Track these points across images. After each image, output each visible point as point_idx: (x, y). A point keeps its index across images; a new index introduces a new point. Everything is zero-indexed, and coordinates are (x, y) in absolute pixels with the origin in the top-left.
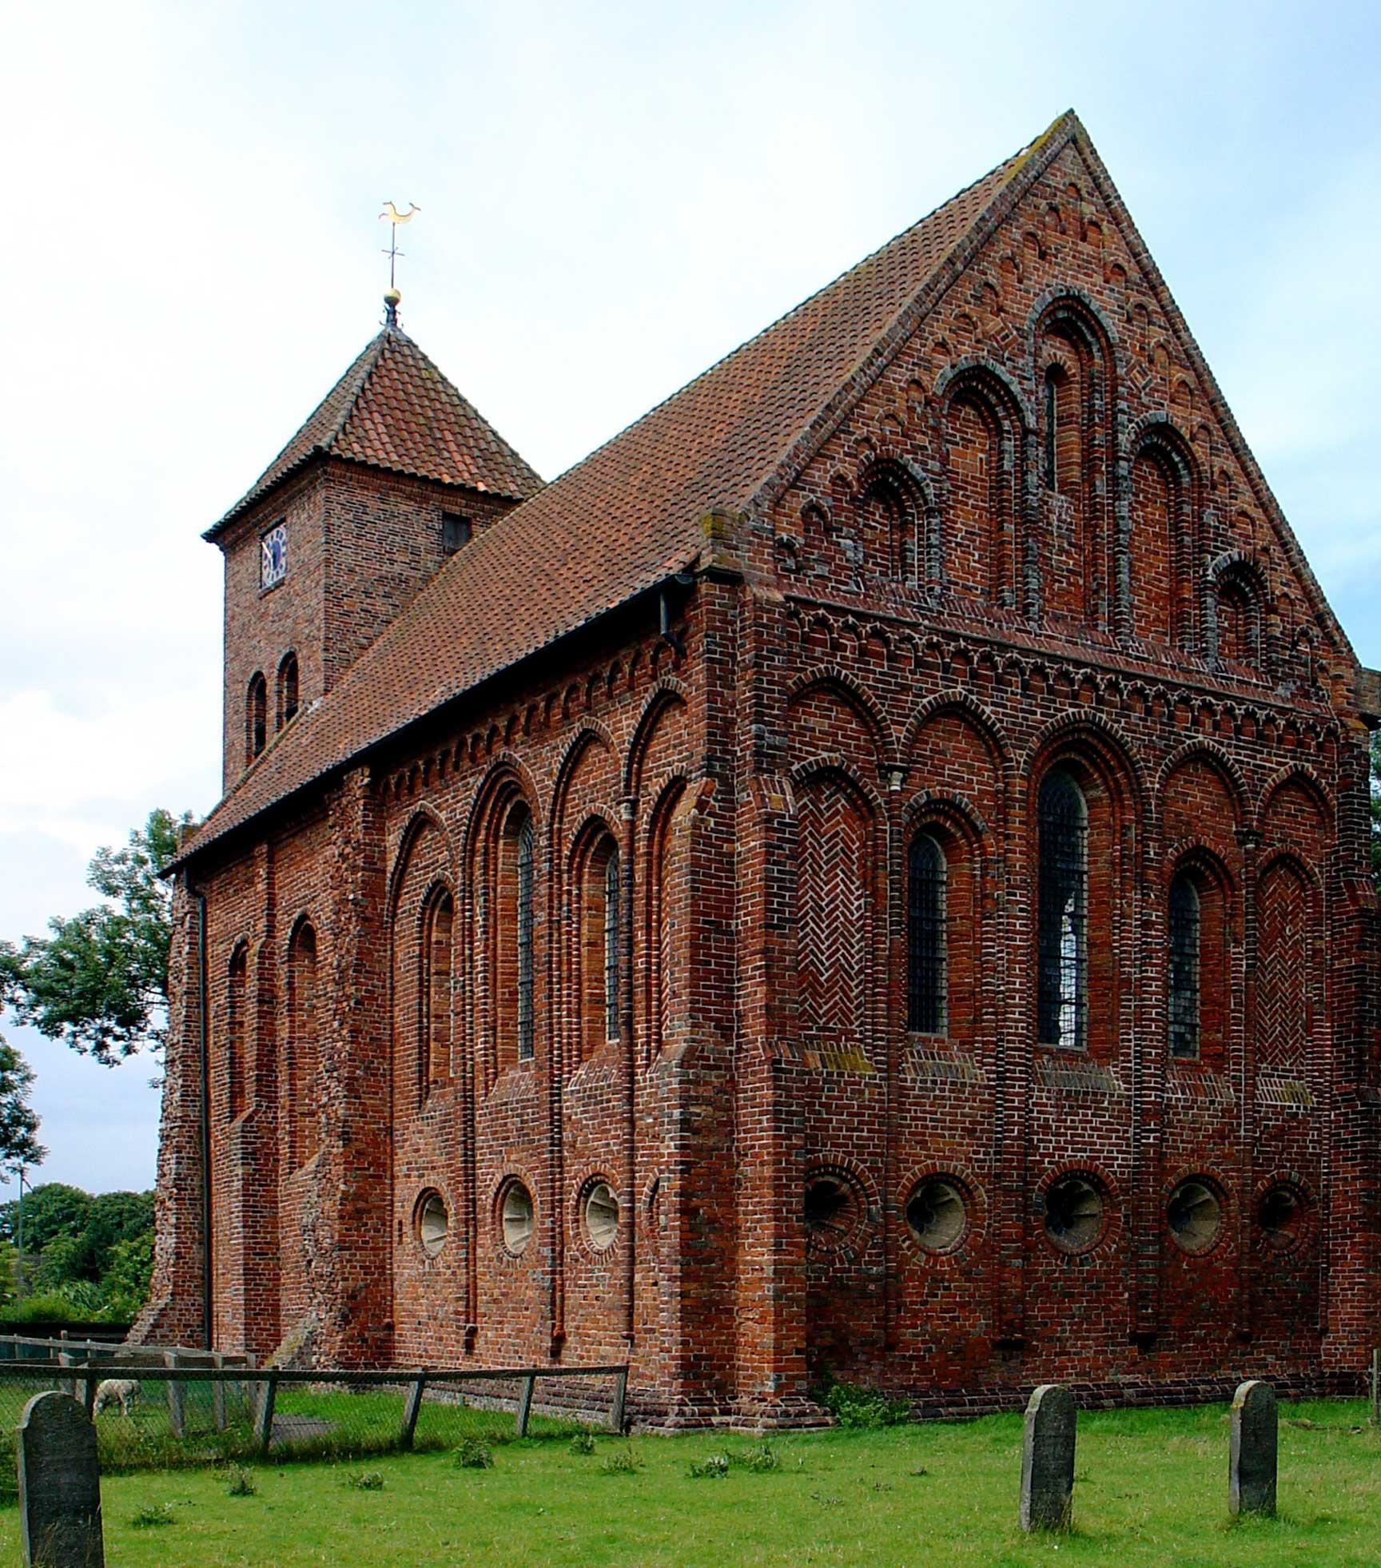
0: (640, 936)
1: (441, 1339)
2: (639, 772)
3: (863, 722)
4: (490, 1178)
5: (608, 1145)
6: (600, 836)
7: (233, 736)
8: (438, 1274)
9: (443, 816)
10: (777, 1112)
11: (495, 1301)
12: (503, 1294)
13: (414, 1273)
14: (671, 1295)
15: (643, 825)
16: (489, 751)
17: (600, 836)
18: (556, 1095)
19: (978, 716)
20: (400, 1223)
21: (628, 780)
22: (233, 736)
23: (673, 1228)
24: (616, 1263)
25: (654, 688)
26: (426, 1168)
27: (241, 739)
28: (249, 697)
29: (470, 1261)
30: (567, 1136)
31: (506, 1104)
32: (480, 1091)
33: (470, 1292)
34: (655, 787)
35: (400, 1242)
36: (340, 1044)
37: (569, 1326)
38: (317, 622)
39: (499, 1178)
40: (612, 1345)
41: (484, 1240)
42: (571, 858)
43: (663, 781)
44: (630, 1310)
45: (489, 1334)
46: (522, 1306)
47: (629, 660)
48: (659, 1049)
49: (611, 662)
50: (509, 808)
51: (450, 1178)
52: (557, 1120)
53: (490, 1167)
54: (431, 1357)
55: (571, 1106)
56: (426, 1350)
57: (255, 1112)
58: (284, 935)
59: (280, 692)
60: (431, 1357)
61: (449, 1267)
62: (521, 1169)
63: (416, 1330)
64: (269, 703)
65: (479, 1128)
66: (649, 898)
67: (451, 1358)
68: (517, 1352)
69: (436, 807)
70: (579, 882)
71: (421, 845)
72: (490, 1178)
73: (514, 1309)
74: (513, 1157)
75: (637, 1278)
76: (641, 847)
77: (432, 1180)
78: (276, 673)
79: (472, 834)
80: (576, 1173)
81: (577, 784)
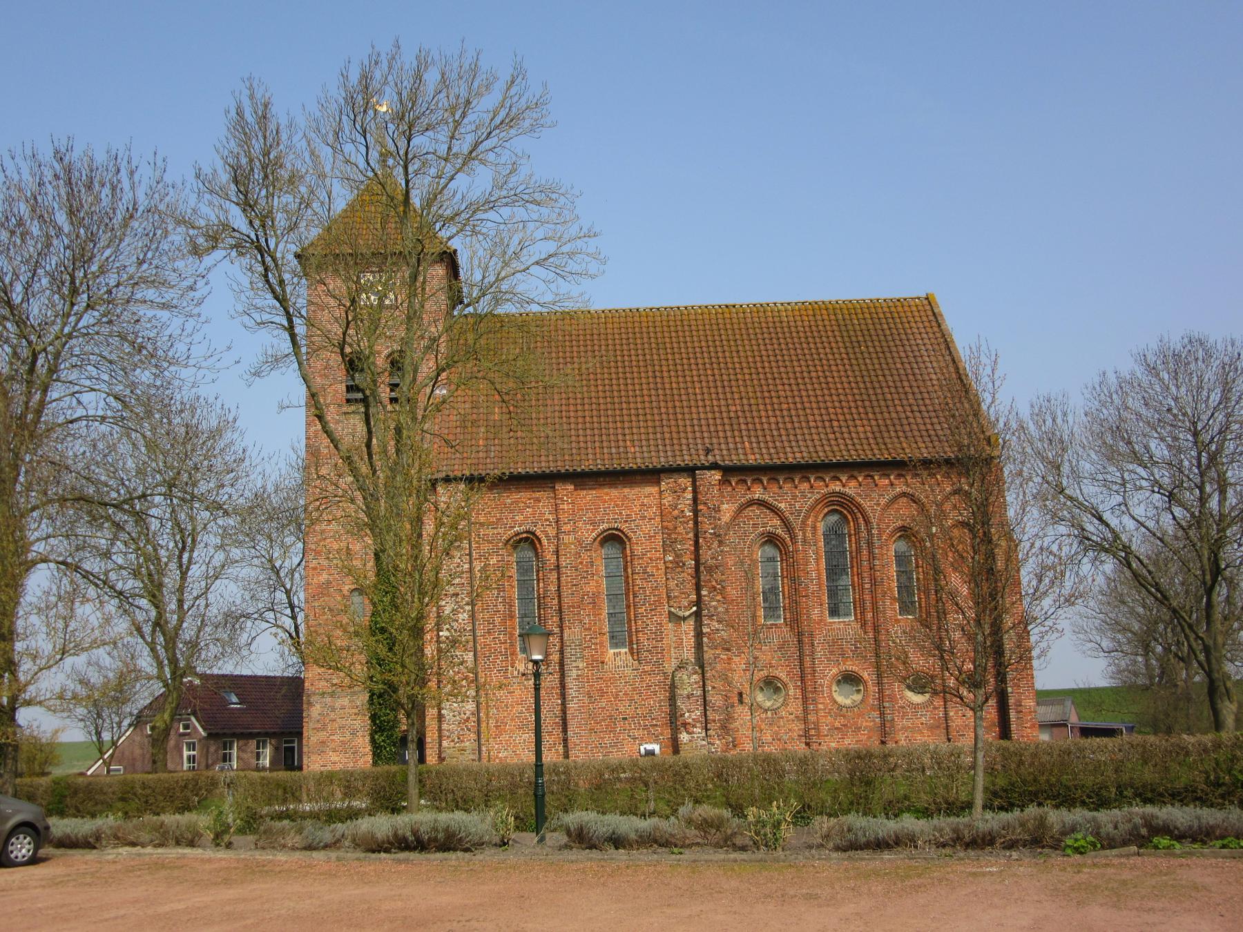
9: (782, 506)
24: (935, 708)
39: (835, 671)
62: (855, 668)
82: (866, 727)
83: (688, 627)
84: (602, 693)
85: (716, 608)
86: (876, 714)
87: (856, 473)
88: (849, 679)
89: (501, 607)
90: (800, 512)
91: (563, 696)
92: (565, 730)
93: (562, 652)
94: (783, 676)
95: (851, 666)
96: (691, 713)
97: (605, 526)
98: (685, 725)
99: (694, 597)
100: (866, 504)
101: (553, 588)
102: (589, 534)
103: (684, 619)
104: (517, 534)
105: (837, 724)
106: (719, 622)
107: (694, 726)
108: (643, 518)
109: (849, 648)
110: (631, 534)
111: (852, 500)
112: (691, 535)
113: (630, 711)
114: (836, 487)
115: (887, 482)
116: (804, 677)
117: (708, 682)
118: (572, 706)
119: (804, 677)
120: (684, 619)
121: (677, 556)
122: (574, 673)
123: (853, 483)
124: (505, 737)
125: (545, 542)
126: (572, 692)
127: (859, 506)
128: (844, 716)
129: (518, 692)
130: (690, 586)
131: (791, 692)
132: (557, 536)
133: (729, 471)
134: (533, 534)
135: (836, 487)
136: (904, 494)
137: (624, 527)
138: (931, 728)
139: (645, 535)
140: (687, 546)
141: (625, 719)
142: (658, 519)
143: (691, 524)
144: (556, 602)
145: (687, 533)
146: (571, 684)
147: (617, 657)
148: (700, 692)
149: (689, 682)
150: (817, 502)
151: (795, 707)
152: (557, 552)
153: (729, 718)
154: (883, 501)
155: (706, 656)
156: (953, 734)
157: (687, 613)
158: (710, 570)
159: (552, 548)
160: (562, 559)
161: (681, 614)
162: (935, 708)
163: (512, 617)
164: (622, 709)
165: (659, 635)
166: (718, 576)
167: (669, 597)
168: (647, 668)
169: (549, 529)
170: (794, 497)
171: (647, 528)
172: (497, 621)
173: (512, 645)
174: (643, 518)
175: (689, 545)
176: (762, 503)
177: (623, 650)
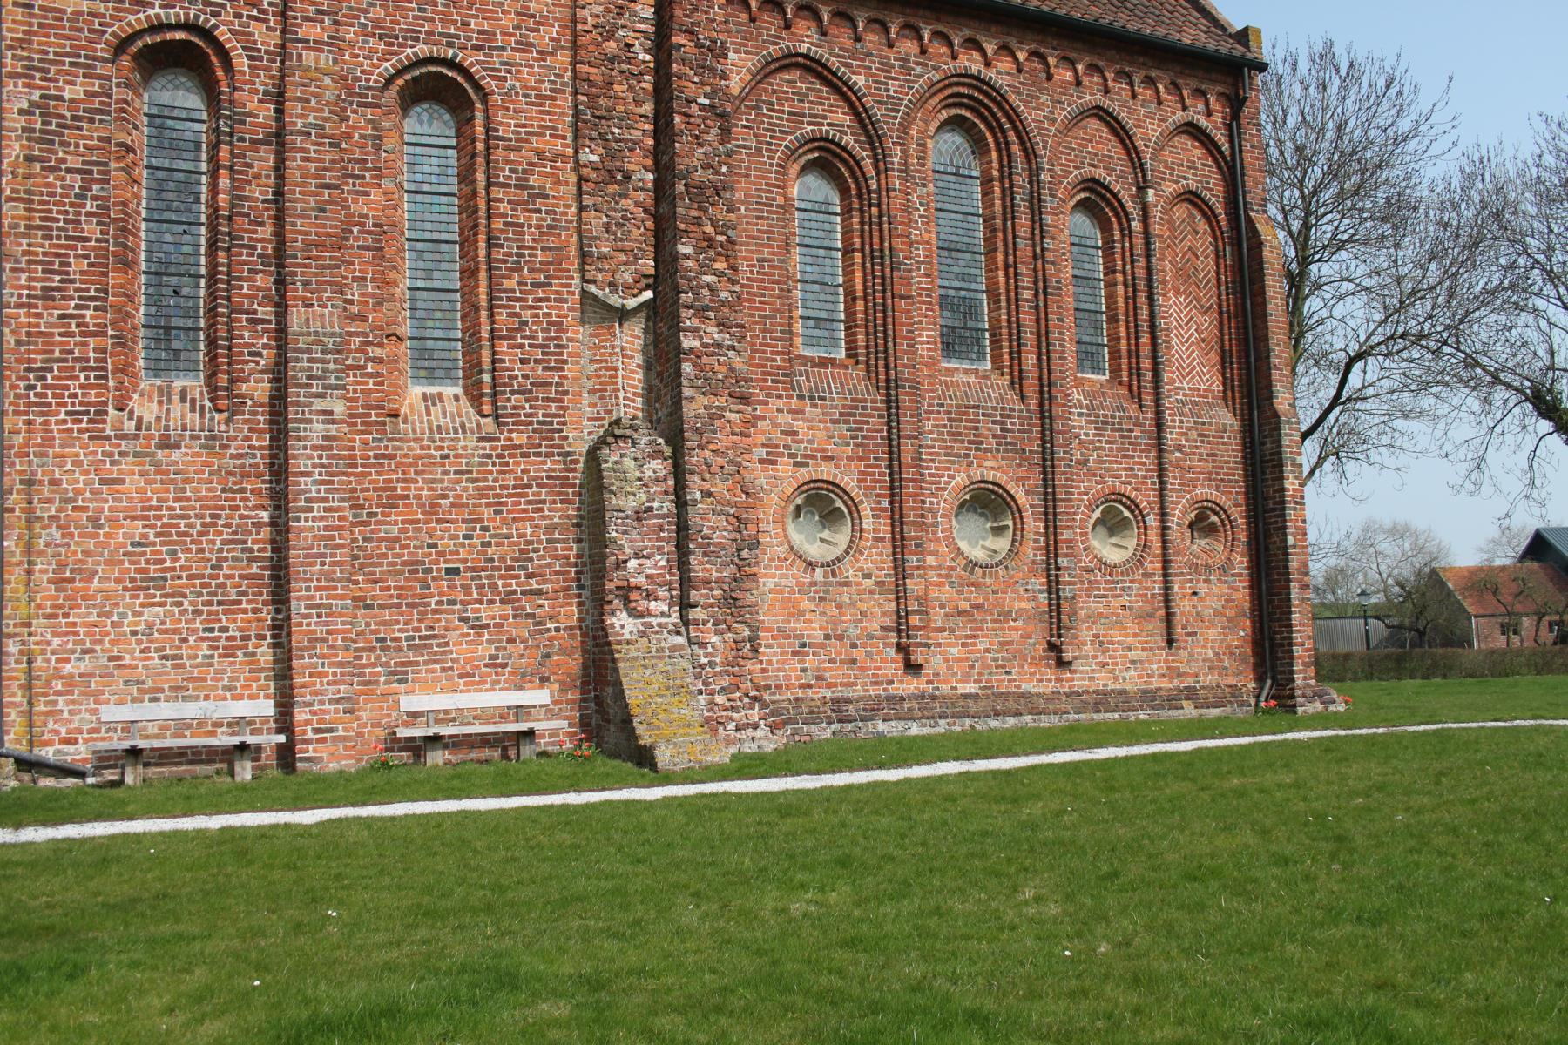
1: (854, 662)
5: (1132, 469)
8: (847, 584)
9: (860, 80)
11: (961, 614)
12: (977, 607)
13: (791, 582)
24: (1146, 575)
26: (813, 457)
31: (978, 407)
39: (961, 479)
40: (1144, 650)
44: (1169, 616)
51: (861, 473)
53: (949, 469)
54: (829, 686)
56: (819, 678)
60: (829, 686)
61: (869, 576)
62: (1002, 478)
63: (795, 653)
67: (876, 683)
68: (1003, 666)
73: (995, 621)
74: (988, 463)
77: (826, 471)
82: (1020, 612)
83: (631, 338)
84: (392, 500)
86: (1039, 583)
87: (1013, 43)
88: (987, 502)
89: (91, 228)
91: (280, 501)
92: (280, 597)
93: (280, 376)
94: (849, 482)
95: (992, 469)
96: (643, 559)
97: (422, 50)
98: (626, 592)
99: (648, 264)
100: (1031, 115)
101: (259, 193)
102: (375, 65)
103: (623, 315)
105: (964, 605)
106: (723, 326)
107: (650, 596)
108: (525, 47)
109: (988, 429)
110: (488, 83)
111: (1001, 100)
112: (648, 108)
113: (468, 553)
114: (972, 63)
115: (1068, 76)
116: (895, 488)
117: (693, 480)
118: (307, 528)
119: (895, 488)
120: (623, 315)
121: (610, 155)
122: (318, 428)
123: (1005, 64)
124: (84, 614)
125: (242, 63)
126: (307, 484)
127: (1013, 116)
128: (976, 585)
129: (133, 483)
130: (639, 233)
131: (868, 523)
132: (282, 52)
134: (207, 34)
135: (972, 63)
140: (636, 134)
141: (456, 572)
142: (564, 57)
143: (648, 82)
144: (266, 232)
145: (638, 103)
146: (304, 458)
147: (432, 405)
148: (667, 506)
149: (638, 475)
151: (876, 559)
152: (279, 98)
153: (744, 576)
154: (1060, 116)
155: (689, 410)
156: (1179, 631)
157: (631, 303)
158: (699, 193)
159: (263, 83)
160: (293, 110)
161: (615, 300)
162: (1146, 575)
163: (126, 264)
164: (446, 544)
165: (552, 354)
166: (718, 212)
167: (584, 256)
168: (519, 438)
169: (257, 30)
170: (886, 67)
171: (532, 74)
172: (77, 265)
173: (121, 342)
174: (525, 47)
175: (642, 132)
176: (814, 68)
177: (450, 390)
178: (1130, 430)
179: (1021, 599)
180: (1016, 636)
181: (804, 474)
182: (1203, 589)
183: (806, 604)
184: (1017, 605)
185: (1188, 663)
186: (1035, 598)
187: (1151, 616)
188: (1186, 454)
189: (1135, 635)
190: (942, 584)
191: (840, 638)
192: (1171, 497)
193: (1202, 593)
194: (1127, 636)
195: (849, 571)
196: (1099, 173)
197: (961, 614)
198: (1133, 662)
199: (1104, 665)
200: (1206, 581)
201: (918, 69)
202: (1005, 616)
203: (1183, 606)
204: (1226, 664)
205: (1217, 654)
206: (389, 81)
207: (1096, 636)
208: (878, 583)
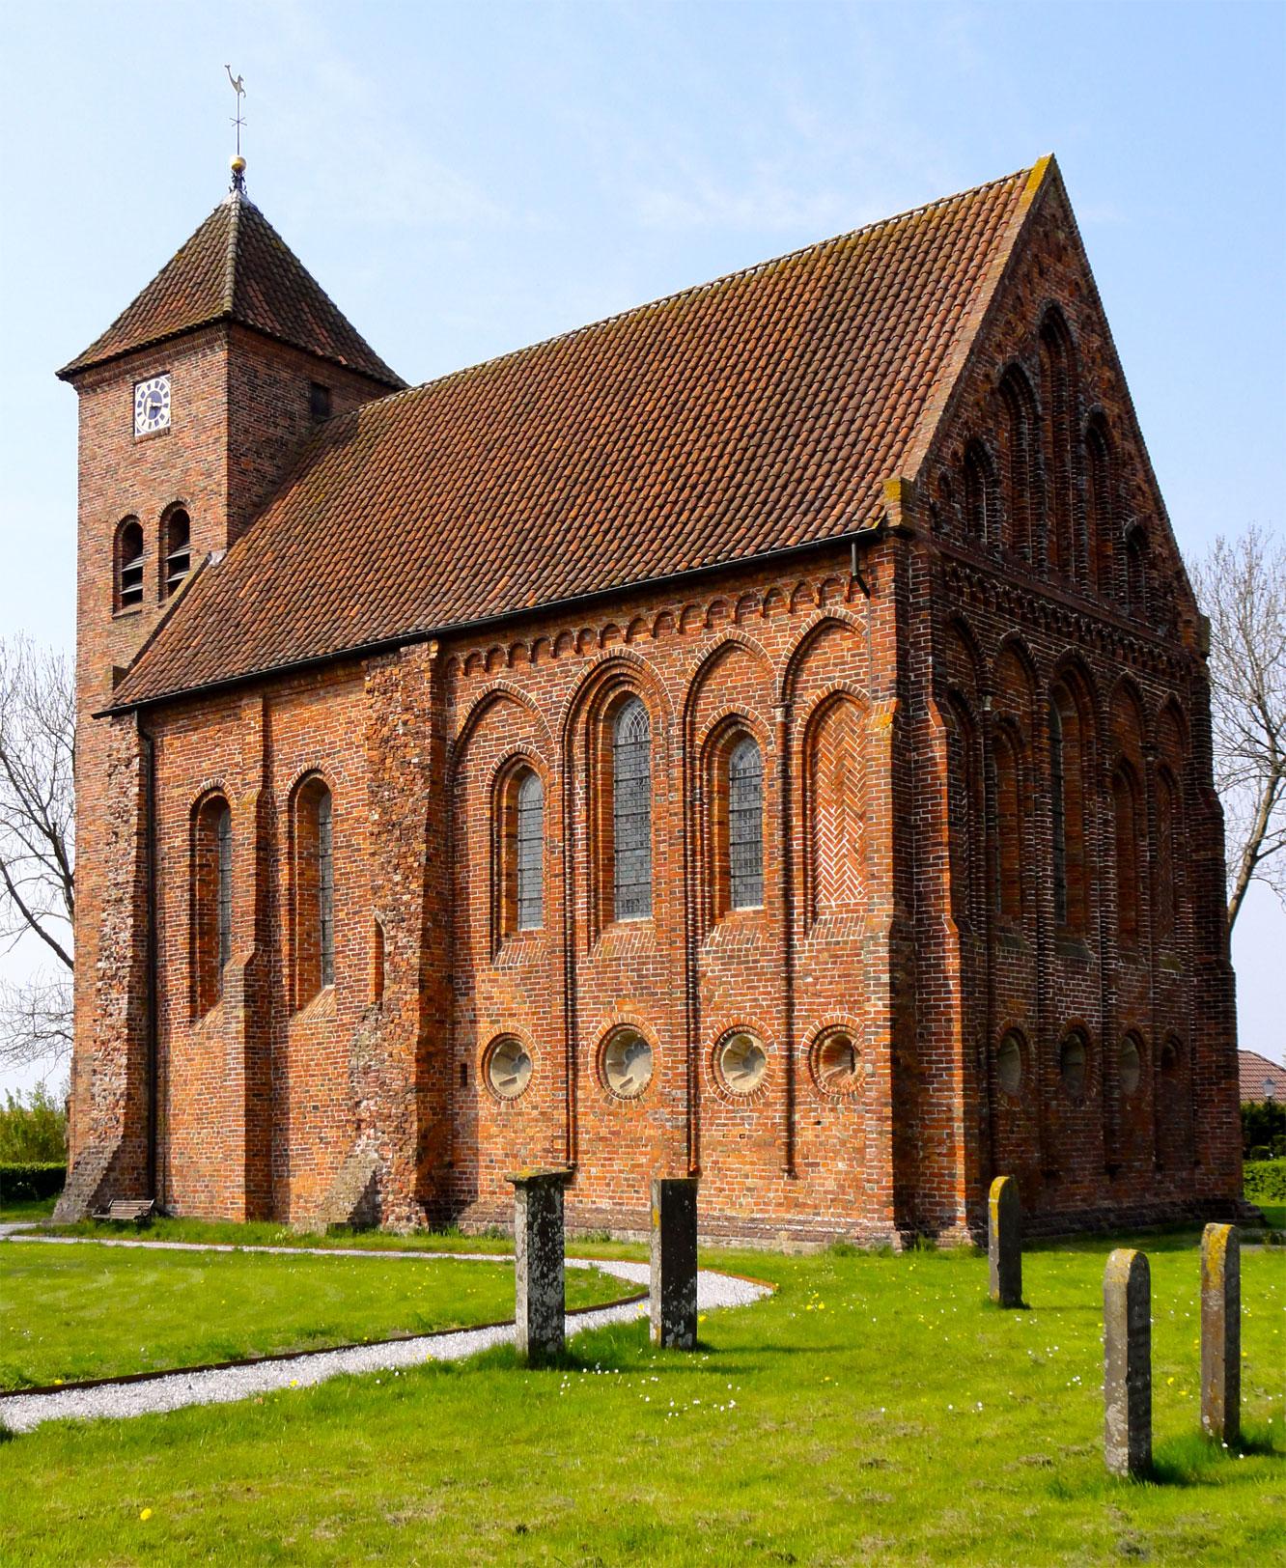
0: (796, 822)
2: (794, 682)
3: (970, 656)
4: (594, 1026)
6: (730, 732)
7: (92, 572)
8: (520, 1114)
9: (532, 696)
10: (962, 978)
12: (613, 1133)
14: (880, 1133)
15: (797, 728)
16: (602, 646)
17: (730, 732)
18: (692, 955)
19: (1025, 649)
20: (464, 1067)
21: (784, 688)
22: (92, 572)
23: (882, 1075)
24: (767, 1104)
25: (817, 615)
27: (105, 578)
28: (116, 538)
29: (571, 1103)
30: (703, 991)
32: (581, 945)
33: (571, 1131)
34: (809, 697)
35: (465, 1084)
36: (405, 898)
37: (706, 1162)
38: (216, 477)
39: (606, 1025)
41: (587, 1081)
42: (704, 748)
43: (822, 693)
44: (790, 1147)
45: (593, 1170)
46: (635, 1142)
47: (792, 588)
48: (815, 920)
49: (768, 587)
50: (612, 696)
52: (693, 977)
55: (707, 963)
57: (254, 956)
58: (283, 787)
59: (161, 538)
61: (535, 1108)
64: (147, 547)
65: (580, 980)
66: (804, 790)
69: (524, 687)
70: (709, 769)
71: (491, 717)
72: (594, 1026)
74: (627, 1008)
75: (797, 1117)
76: (796, 746)
77: (509, 1025)
78: (157, 520)
79: (572, 716)
80: (712, 1025)
81: (712, 684)
82: (649, 1139)
85: (408, 905)
87: (643, 611)
90: (557, 704)
95: (629, 1013)
97: (303, 767)
100: (662, 673)
104: (206, 793)
105: (604, 1132)
109: (626, 977)
114: (616, 646)
121: (385, 812)
128: (615, 1115)
133: (449, 638)
136: (728, 647)
137: (324, 764)
138: (760, 1145)
139: (348, 778)
141: (315, 1108)
150: (589, 682)
154: (692, 666)
156: (798, 1160)
162: (767, 1104)
164: (313, 1091)
178: (756, 961)
179: (652, 1127)
180: (643, 1160)
181: (496, 1030)
182: (828, 1119)
183: (494, 1130)
184: (647, 1132)
185: (810, 1193)
186: (663, 1126)
187: (772, 1144)
188: (816, 978)
189: (752, 1163)
190: (585, 1114)
191: (515, 1156)
192: (799, 1025)
193: (826, 1121)
194: (744, 1163)
195: (523, 1105)
196: (738, 706)
197: (602, 1139)
198: (749, 1189)
199: (722, 1190)
200: (832, 1110)
201: (574, 669)
202: (635, 1142)
203: (805, 1135)
204: (851, 1197)
205: (841, 1187)
206: (293, 792)
207: (716, 1162)
208: (542, 1113)
